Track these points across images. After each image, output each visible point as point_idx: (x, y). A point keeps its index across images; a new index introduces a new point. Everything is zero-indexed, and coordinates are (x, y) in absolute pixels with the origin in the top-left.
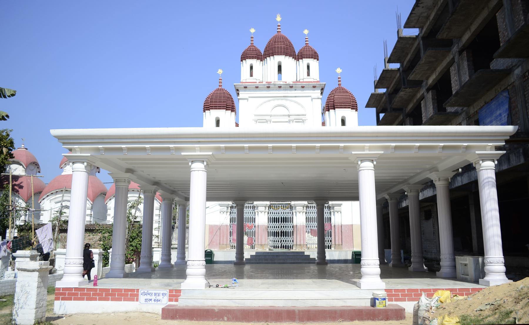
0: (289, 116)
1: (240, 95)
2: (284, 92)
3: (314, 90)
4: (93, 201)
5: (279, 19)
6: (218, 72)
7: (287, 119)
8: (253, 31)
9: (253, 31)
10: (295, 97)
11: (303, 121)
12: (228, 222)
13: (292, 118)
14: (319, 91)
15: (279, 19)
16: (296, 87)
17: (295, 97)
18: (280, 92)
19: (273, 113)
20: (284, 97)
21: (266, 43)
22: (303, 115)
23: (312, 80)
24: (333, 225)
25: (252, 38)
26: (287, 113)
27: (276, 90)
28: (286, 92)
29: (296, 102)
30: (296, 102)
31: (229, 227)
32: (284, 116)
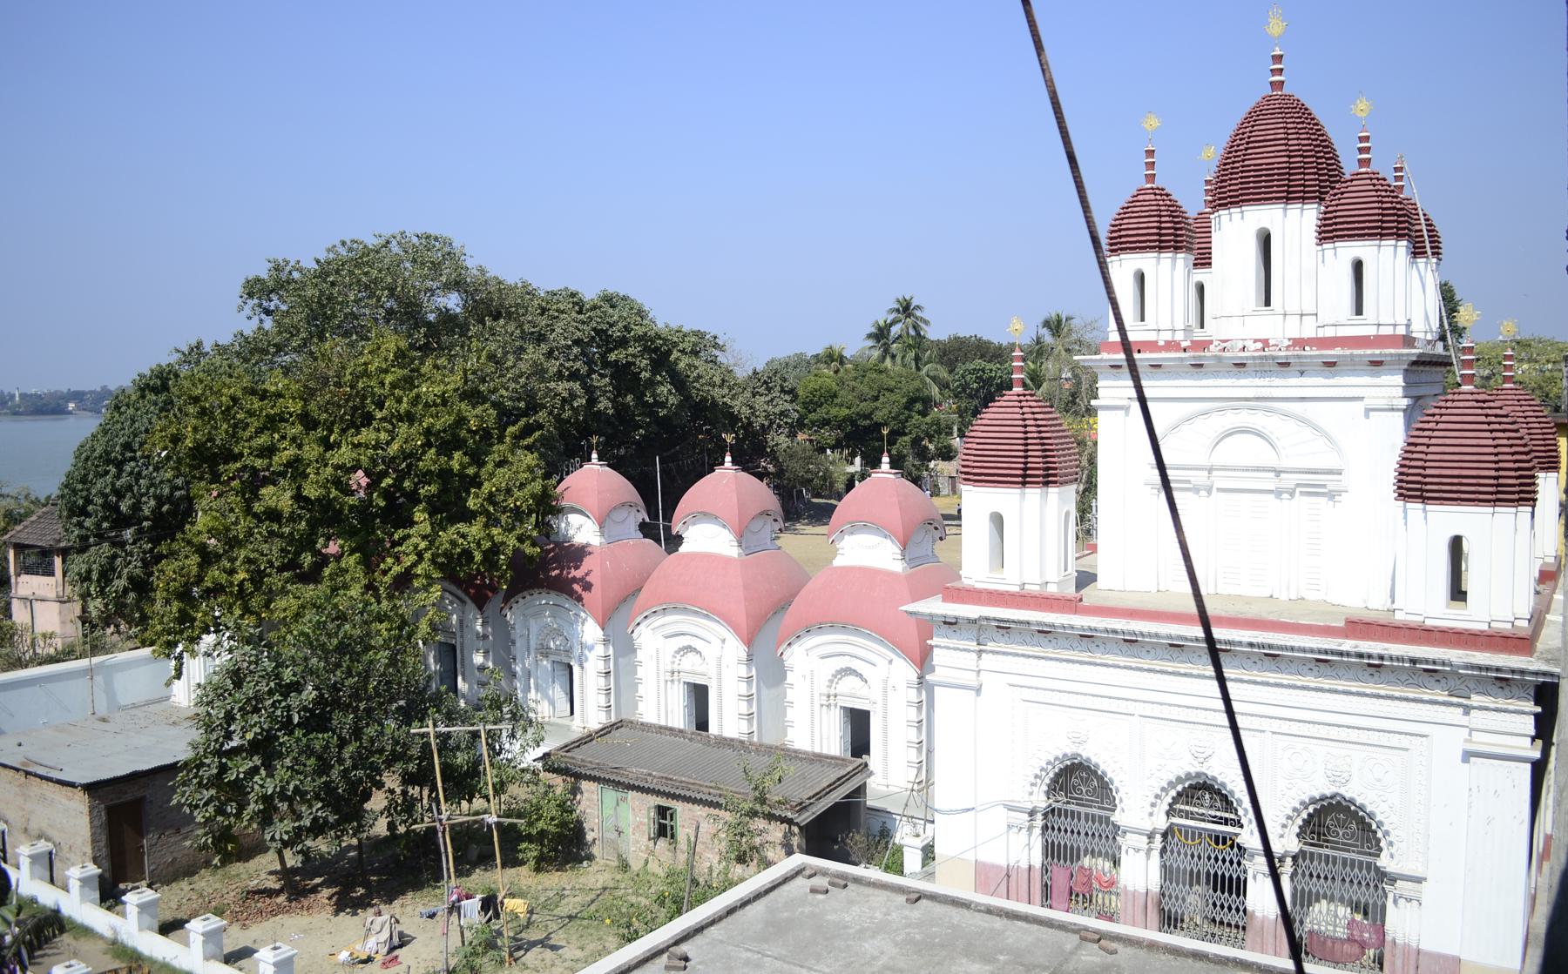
0: (1278, 472)
1: (1101, 392)
2: (1257, 381)
3: (1377, 375)
4: (749, 642)
5: (1276, 27)
6: (1012, 328)
7: (1269, 482)
8: (1152, 122)
9: (1152, 122)
10: (1303, 399)
11: (1332, 495)
12: (1037, 859)
13: (1289, 480)
14: (1399, 379)
15: (1276, 27)
16: (1302, 364)
17: (1303, 399)
18: (1243, 382)
19: (1219, 458)
20: (1258, 399)
21: (1224, 140)
22: (1330, 472)
23: (1371, 331)
24: (1388, 938)
25: (1150, 153)
26: (1268, 458)
27: (1228, 374)
28: (1266, 381)
29: (1303, 420)
30: (1303, 420)
31: (1036, 876)
32: (1258, 469)
